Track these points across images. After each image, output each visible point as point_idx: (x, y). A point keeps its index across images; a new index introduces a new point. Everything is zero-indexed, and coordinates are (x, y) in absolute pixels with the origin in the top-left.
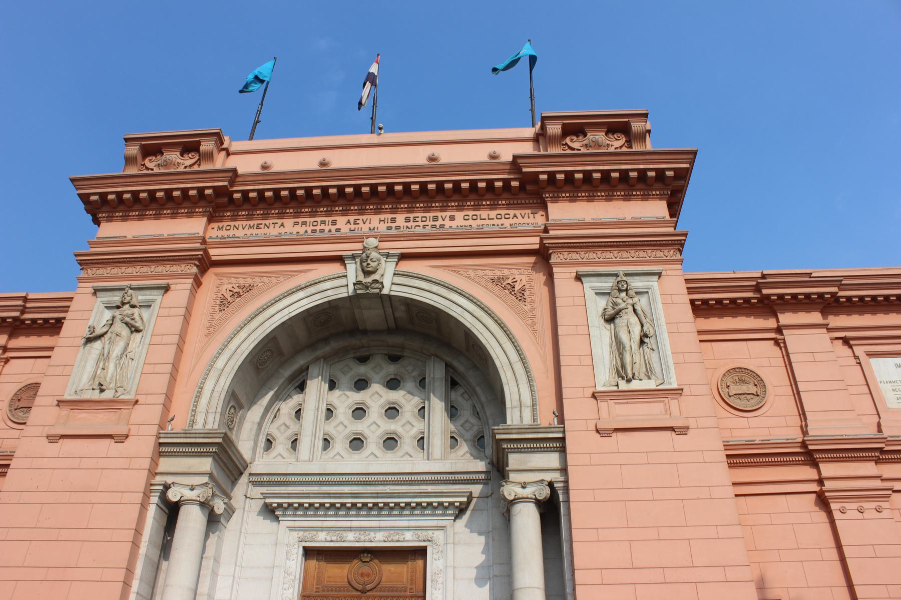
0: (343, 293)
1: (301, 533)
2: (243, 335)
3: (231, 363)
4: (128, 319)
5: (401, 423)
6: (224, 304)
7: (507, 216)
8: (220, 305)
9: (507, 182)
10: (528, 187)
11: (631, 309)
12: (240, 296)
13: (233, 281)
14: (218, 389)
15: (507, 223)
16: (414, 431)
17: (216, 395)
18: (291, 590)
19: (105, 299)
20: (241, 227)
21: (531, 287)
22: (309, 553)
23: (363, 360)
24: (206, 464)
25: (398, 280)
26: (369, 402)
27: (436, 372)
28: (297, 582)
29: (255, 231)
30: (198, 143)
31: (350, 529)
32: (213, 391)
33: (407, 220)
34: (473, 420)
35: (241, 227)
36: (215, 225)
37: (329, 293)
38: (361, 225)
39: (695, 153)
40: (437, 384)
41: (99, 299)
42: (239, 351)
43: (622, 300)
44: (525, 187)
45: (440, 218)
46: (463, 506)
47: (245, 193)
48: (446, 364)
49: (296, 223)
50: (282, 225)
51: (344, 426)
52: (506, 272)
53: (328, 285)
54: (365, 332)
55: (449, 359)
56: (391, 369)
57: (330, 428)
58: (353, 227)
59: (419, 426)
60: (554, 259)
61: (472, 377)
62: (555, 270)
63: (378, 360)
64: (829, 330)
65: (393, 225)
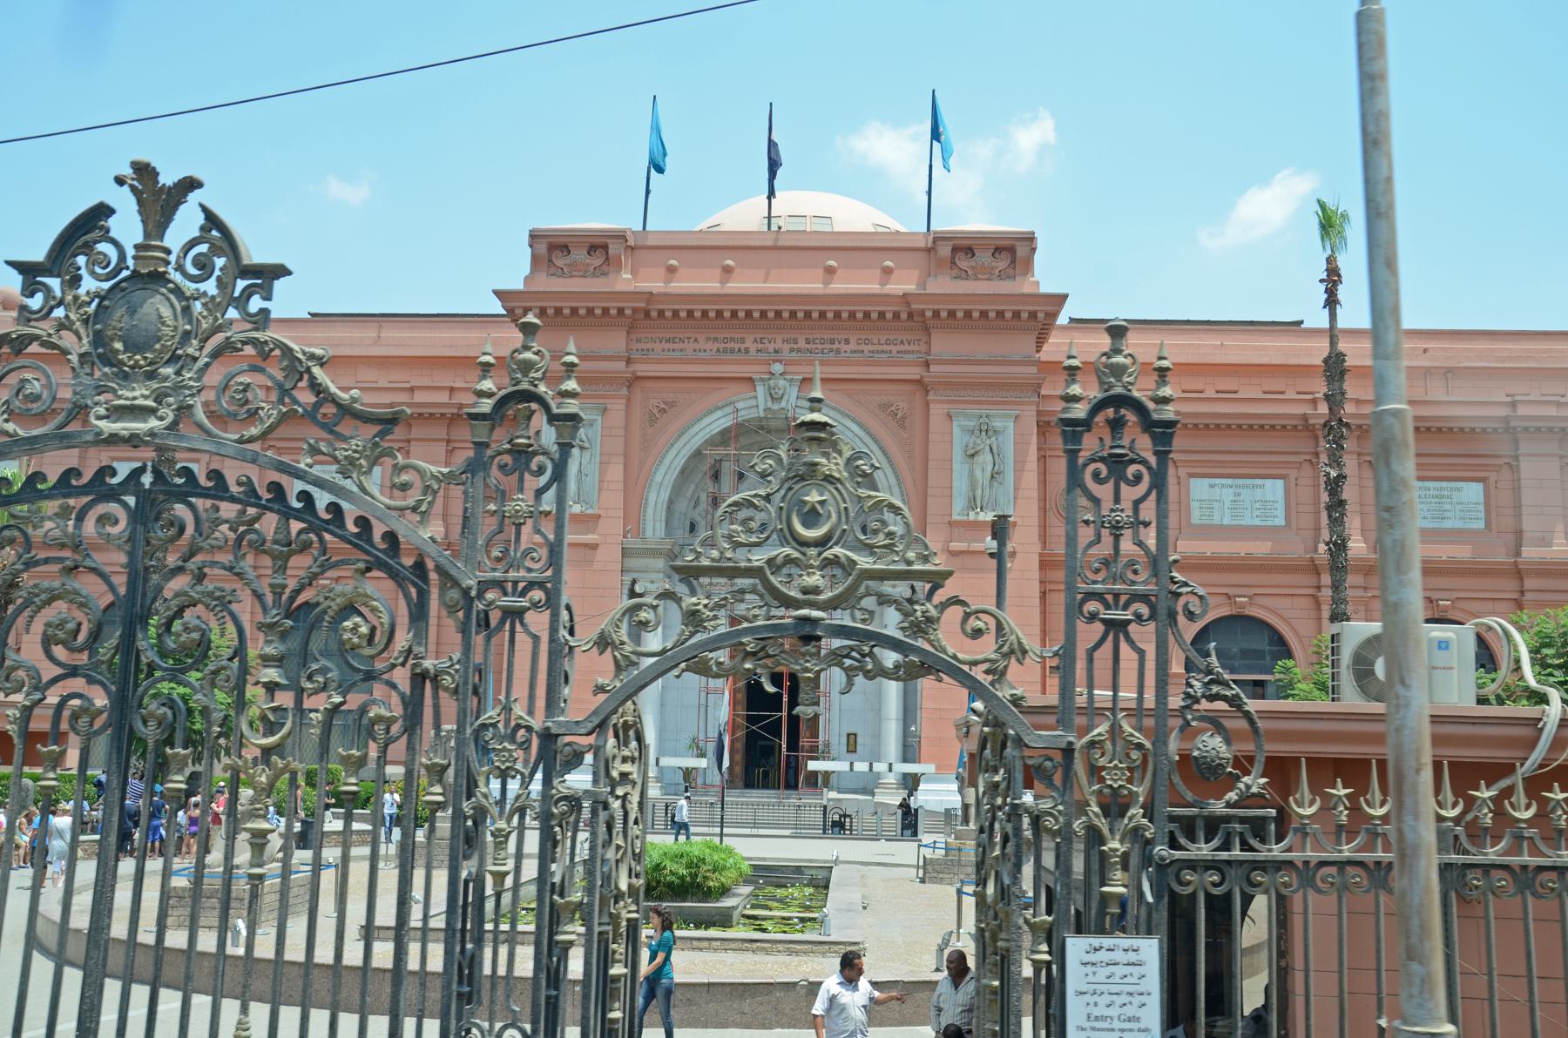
0: (753, 414)
2: (674, 451)
6: (653, 420)
9: (896, 315)
12: (664, 411)
15: (894, 349)
33: (808, 341)
36: (633, 336)
39: (1065, 297)
43: (983, 443)
44: (915, 318)
47: (661, 313)
49: (708, 339)
58: (760, 346)
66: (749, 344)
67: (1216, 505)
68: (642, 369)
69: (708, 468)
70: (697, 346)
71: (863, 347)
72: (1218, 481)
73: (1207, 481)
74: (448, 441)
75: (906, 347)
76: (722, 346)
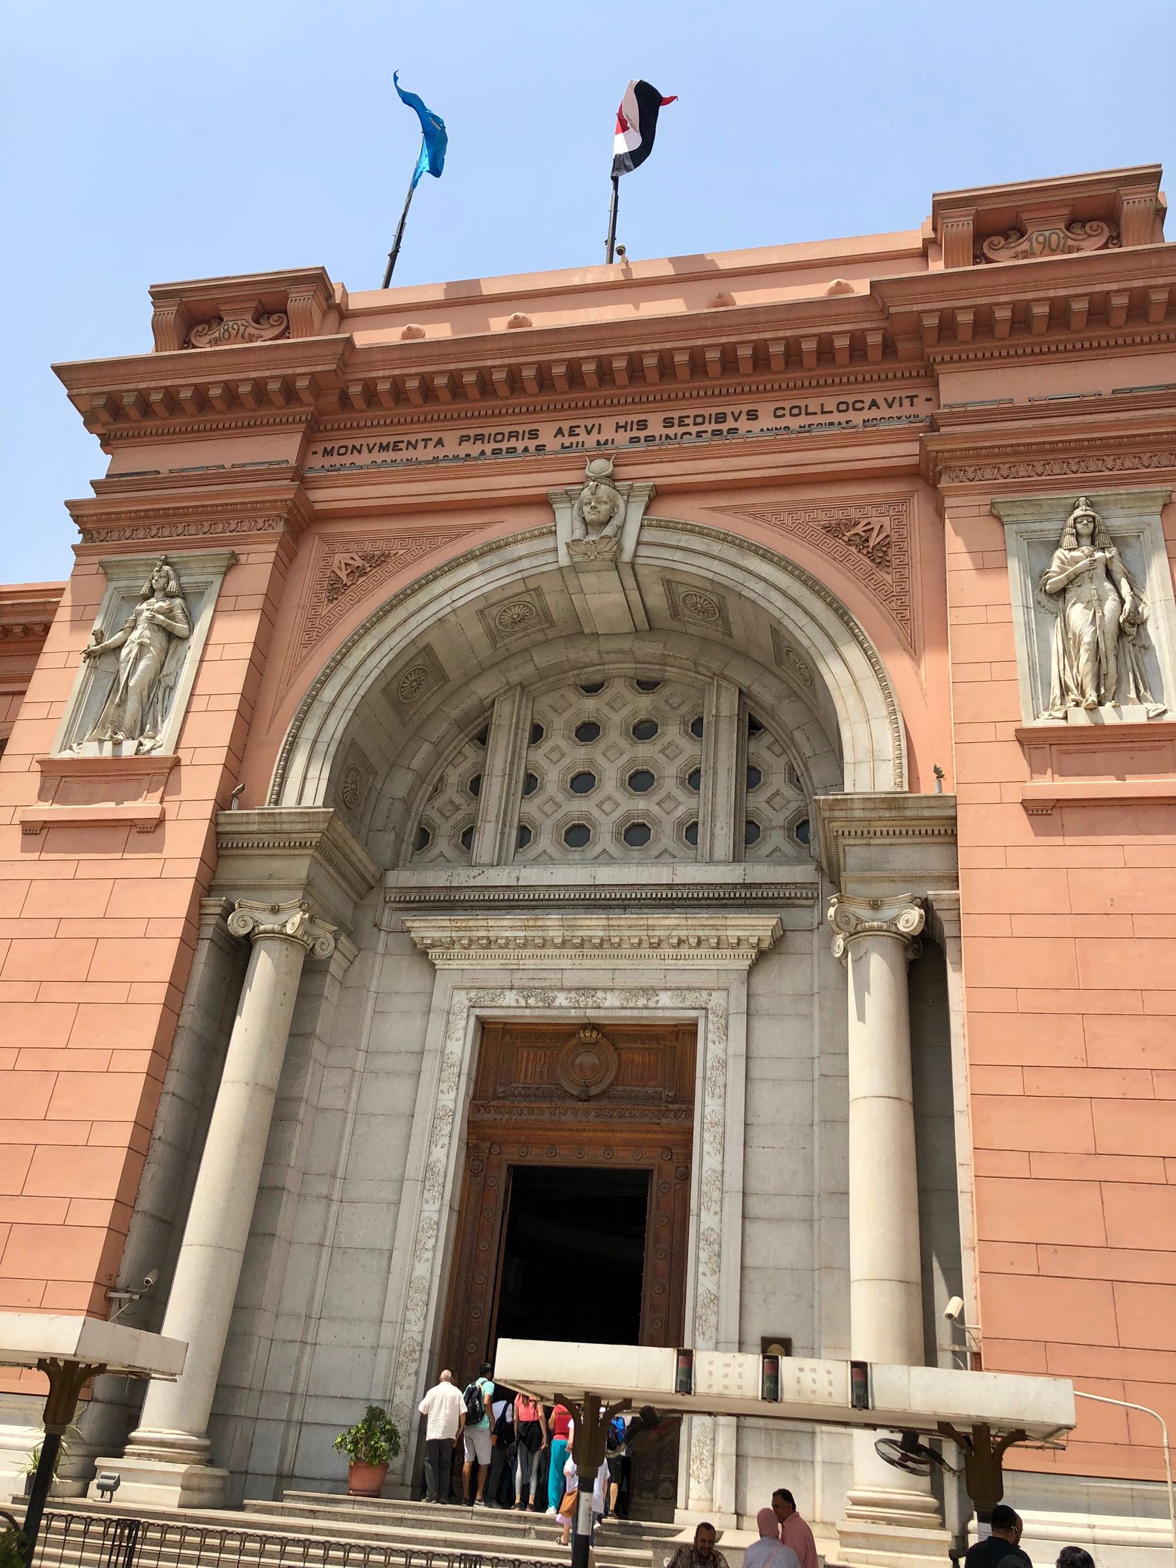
1: (473, 994)
2: (369, 642)
3: (350, 691)
5: (656, 798)
6: (336, 589)
7: (858, 405)
8: (330, 591)
10: (903, 346)
11: (1101, 571)
13: (353, 547)
15: (857, 418)
16: (680, 812)
18: (452, 1094)
19: (123, 583)
20: (365, 448)
21: (902, 538)
22: (484, 1025)
23: (592, 689)
25: (650, 535)
26: (601, 760)
28: (464, 1078)
29: (389, 456)
30: (285, 297)
32: (315, 741)
33: (668, 423)
34: (789, 792)
35: (365, 448)
37: (525, 564)
38: (583, 437)
40: (723, 726)
41: (113, 584)
42: (362, 672)
45: (730, 418)
46: (765, 945)
48: (740, 691)
49: (463, 439)
50: (440, 442)
52: (853, 514)
53: (521, 549)
54: (596, 635)
55: (745, 681)
56: (643, 705)
57: (531, 808)
58: (567, 441)
59: (685, 804)
60: (944, 483)
61: (788, 713)
62: (948, 502)
63: (619, 688)
65: (642, 434)
66: (547, 436)
68: (324, 497)
70: (440, 452)
71: (788, 421)
75: (884, 412)
76: (488, 448)
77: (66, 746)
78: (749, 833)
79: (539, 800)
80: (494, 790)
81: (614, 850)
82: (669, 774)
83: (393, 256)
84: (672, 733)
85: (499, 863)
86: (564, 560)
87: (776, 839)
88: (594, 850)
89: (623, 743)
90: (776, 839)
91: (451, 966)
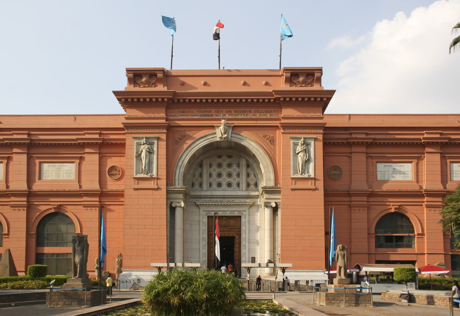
4: (148, 150)
6: (177, 142)
14: (181, 172)
16: (236, 181)
17: (180, 174)
23: (220, 157)
24: (181, 196)
25: (233, 135)
26: (222, 171)
27: (243, 163)
31: (220, 211)
34: (254, 178)
40: (244, 166)
51: (215, 180)
55: (247, 159)
56: (229, 160)
57: (211, 180)
59: (237, 180)
61: (255, 165)
64: (367, 153)
67: (386, 173)
69: (198, 161)
72: (387, 164)
73: (383, 164)
74: (100, 154)
77: (136, 175)
78: (248, 185)
79: (212, 178)
80: (205, 176)
81: (226, 188)
82: (234, 174)
83: (172, 56)
84: (235, 166)
85: (208, 190)
86: (219, 140)
87: (252, 187)
88: (223, 188)
89: (226, 168)
90: (252, 187)
91: (202, 209)
